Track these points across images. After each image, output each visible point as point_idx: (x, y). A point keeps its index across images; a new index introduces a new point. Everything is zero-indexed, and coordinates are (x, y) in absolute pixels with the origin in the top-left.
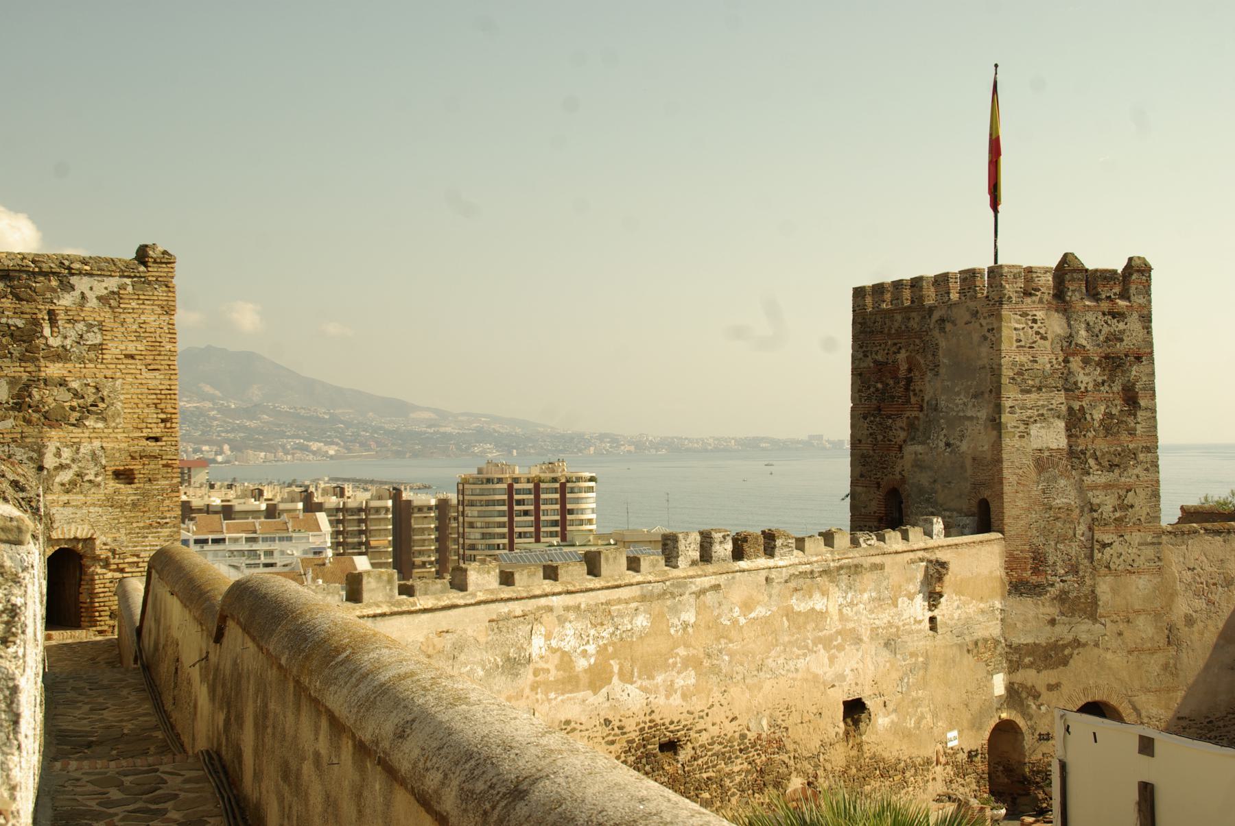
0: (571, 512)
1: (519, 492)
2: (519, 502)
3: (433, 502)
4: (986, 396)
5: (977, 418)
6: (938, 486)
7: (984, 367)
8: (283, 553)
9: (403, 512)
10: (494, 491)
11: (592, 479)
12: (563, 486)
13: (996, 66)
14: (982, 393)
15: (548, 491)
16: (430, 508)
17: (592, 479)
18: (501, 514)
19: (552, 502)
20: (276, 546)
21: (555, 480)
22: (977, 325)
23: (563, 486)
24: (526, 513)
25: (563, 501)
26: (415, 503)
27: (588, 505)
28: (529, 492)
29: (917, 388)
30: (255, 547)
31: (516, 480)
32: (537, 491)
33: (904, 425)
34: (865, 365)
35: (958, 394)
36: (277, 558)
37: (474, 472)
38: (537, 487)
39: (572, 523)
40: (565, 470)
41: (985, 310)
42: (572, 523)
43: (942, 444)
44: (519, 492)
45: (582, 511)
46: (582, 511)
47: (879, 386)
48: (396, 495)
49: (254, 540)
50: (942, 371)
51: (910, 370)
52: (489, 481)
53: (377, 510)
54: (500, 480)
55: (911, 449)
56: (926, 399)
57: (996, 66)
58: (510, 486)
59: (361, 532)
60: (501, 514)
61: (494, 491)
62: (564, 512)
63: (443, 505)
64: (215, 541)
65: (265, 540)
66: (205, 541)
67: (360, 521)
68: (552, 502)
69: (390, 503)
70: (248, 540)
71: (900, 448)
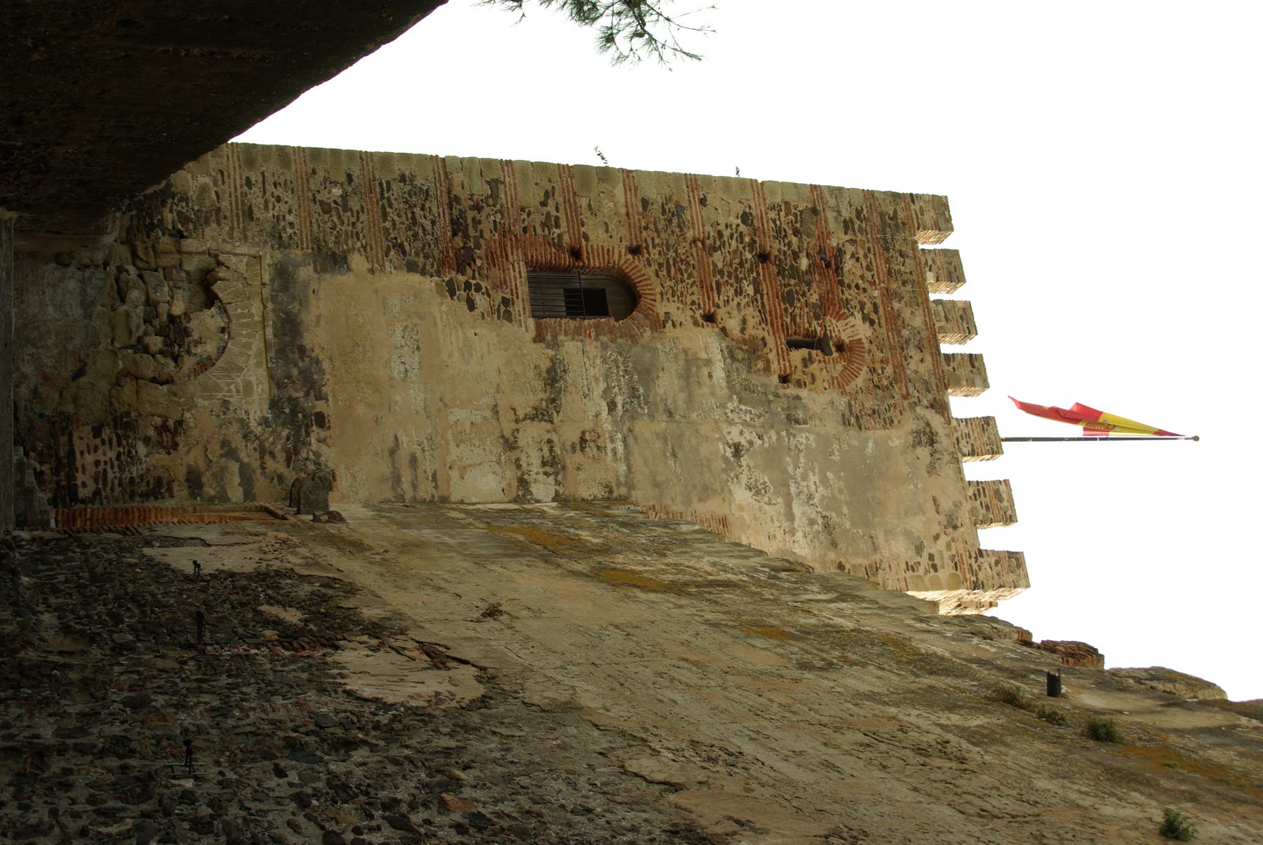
4: (832, 555)
5: (793, 532)
6: (661, 425)
7: (876, 548)
13: (1196, 439)
14: (834, 544)
22: (936, 529)
29: (814, 368)
33: (750, 331)
34: (832, 226)
35: (824, 481)
41: (960, 545)
43: (734, 435)
47: (804, 263)
50: (853, 437)
51: (840, 347)
55: (707, 343)
56: (803, 393)
57: (1196, 439)
71: (710, 318)
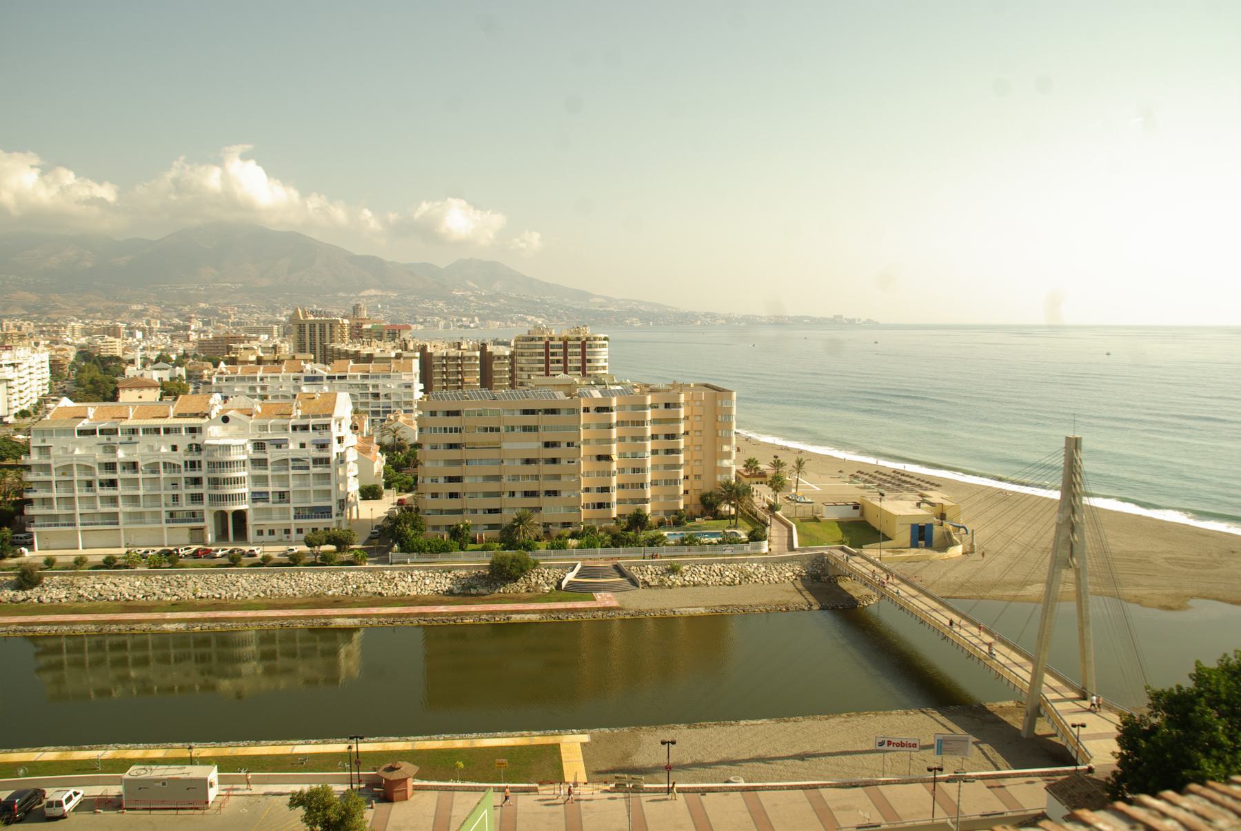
0: (589, 361)
1: (553, 347)
2: (553, 354)
3: (507, 353)
8: (384, 386)
9: (487, 360)
10: (536, 347)
11: (605, 339)
12: (584, 343)
15: (573, 346)
16: (505, 357)
17: (605, 339)
18: (540, 362)
19: (576, 353)
20: (379, 382)
21: (578, 339)
23: (584, 343)
24: (558, 361)
25: (584, 353)
26: (495, 353)
27: (602, 357)
28: (559, 347)
30: (366, 382)
31: (552, 339)
32: (565, 346)
36: (382, 391)
37: (525, 334)
38: (565, 343)
39: (590, 368)
40: (588, 332)
42: (590, 368)
44: (553, 347)
45: (598, 360)
46: (598, 360)
48: (483, 348)
49: (366, 377)
52: (533, 339)
53: (470, 358)
54: (540, 339)
58: (547, 343)
59: (459, 372)
60: (540, 362)
61: (536, 347)
62: (585, 361)
63: (512, 356)
64: (340, 378)
65: (373, 377)
66: (334, 378)
67: (458, 365)
68: (576, 353)
69: (478, 354)
70: (363, 377)
